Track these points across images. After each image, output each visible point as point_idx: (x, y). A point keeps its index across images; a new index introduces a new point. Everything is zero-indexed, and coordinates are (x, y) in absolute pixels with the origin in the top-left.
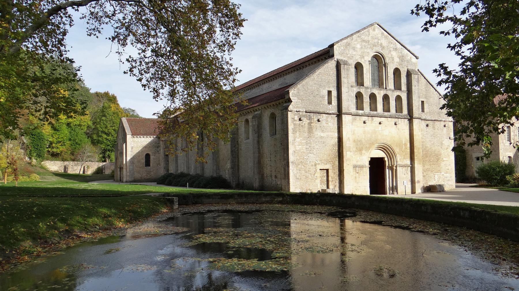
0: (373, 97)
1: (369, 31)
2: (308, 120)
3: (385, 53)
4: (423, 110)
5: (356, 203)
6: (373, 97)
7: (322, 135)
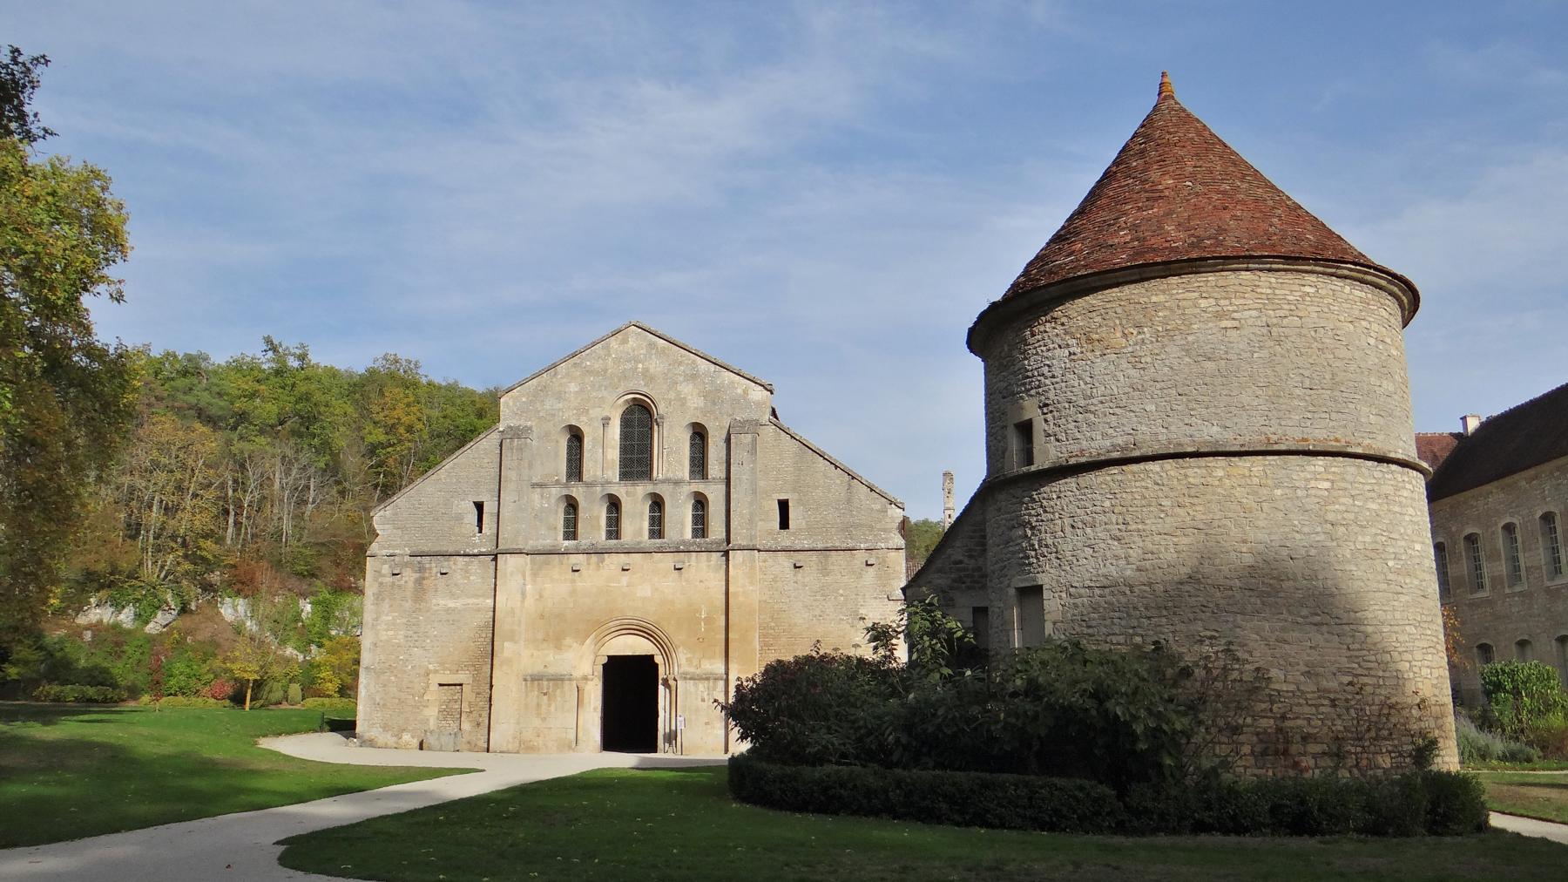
0: (614, 504)
1: (607, 348)
7: (451, 604)
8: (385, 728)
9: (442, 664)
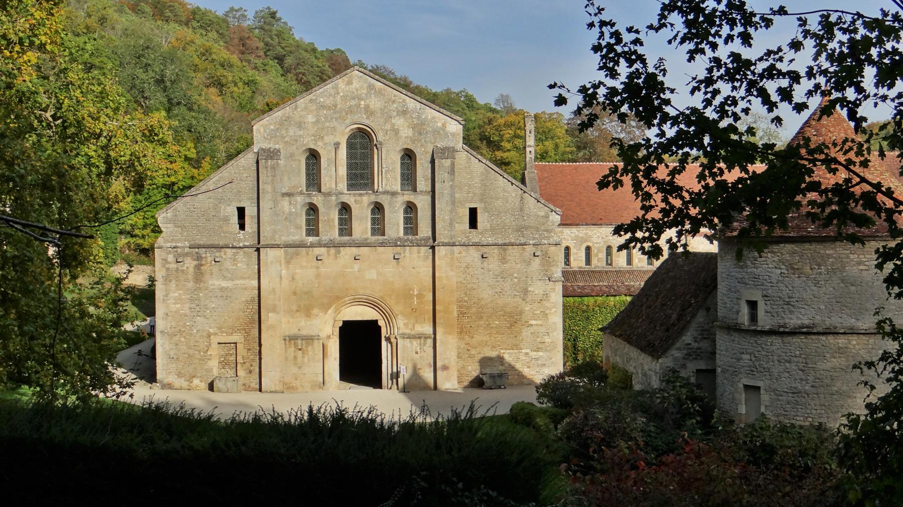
0: (345, 209)
1: (336, 88)
3: (375, 124)
7: (224, 284)
8: (179, 375)
9: (220, 328)
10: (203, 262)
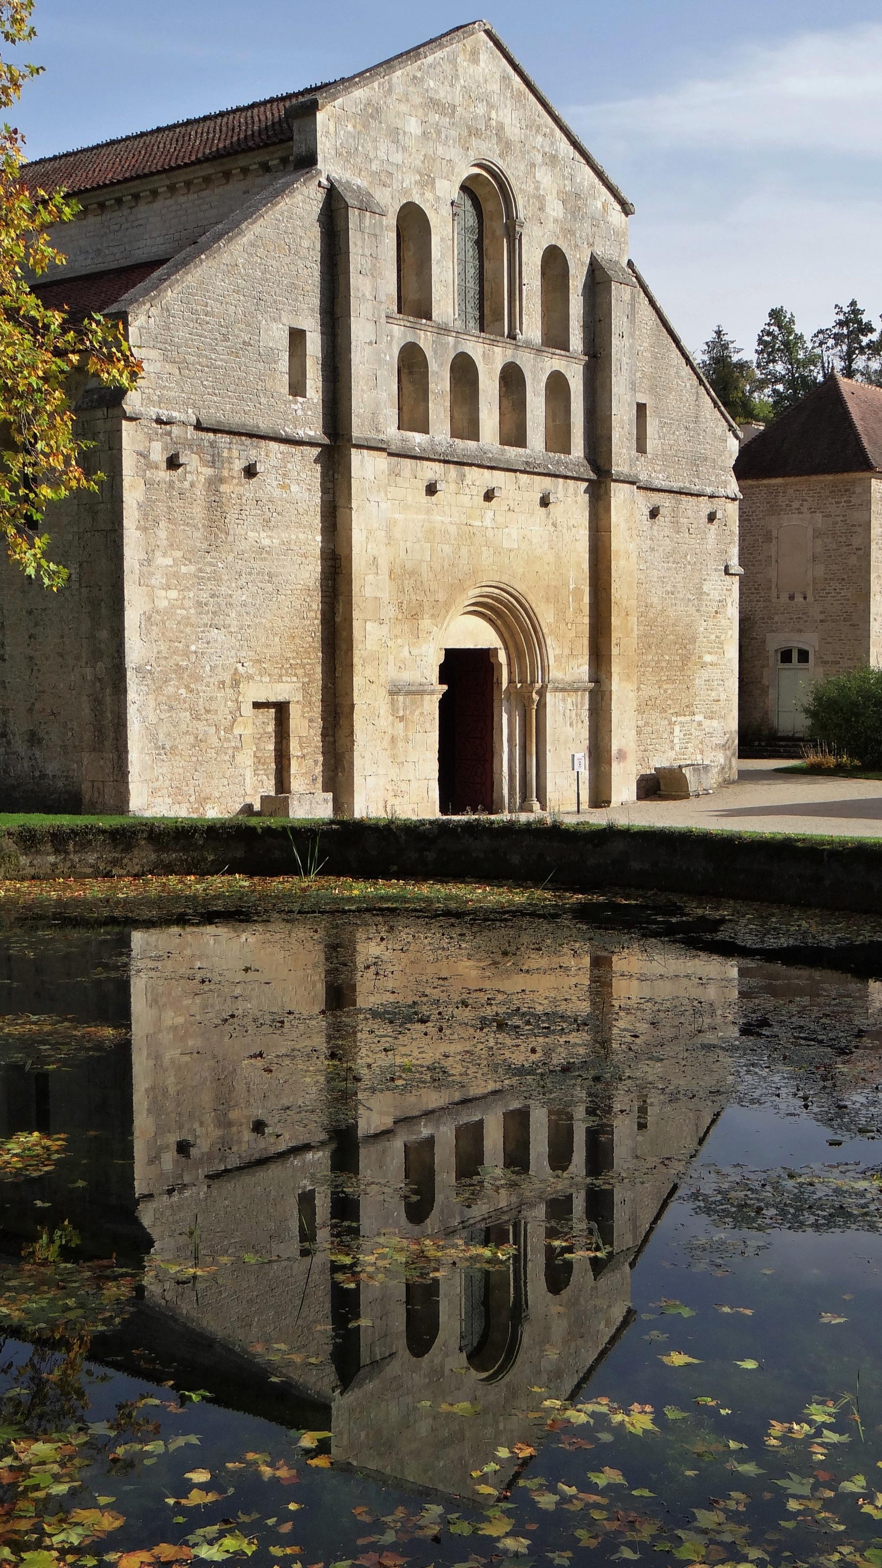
1: (453, 61)
2: (205, 463)
4: (641, 448)
5: (635, 865)
6: (464, 371)
10: (225, 473)
